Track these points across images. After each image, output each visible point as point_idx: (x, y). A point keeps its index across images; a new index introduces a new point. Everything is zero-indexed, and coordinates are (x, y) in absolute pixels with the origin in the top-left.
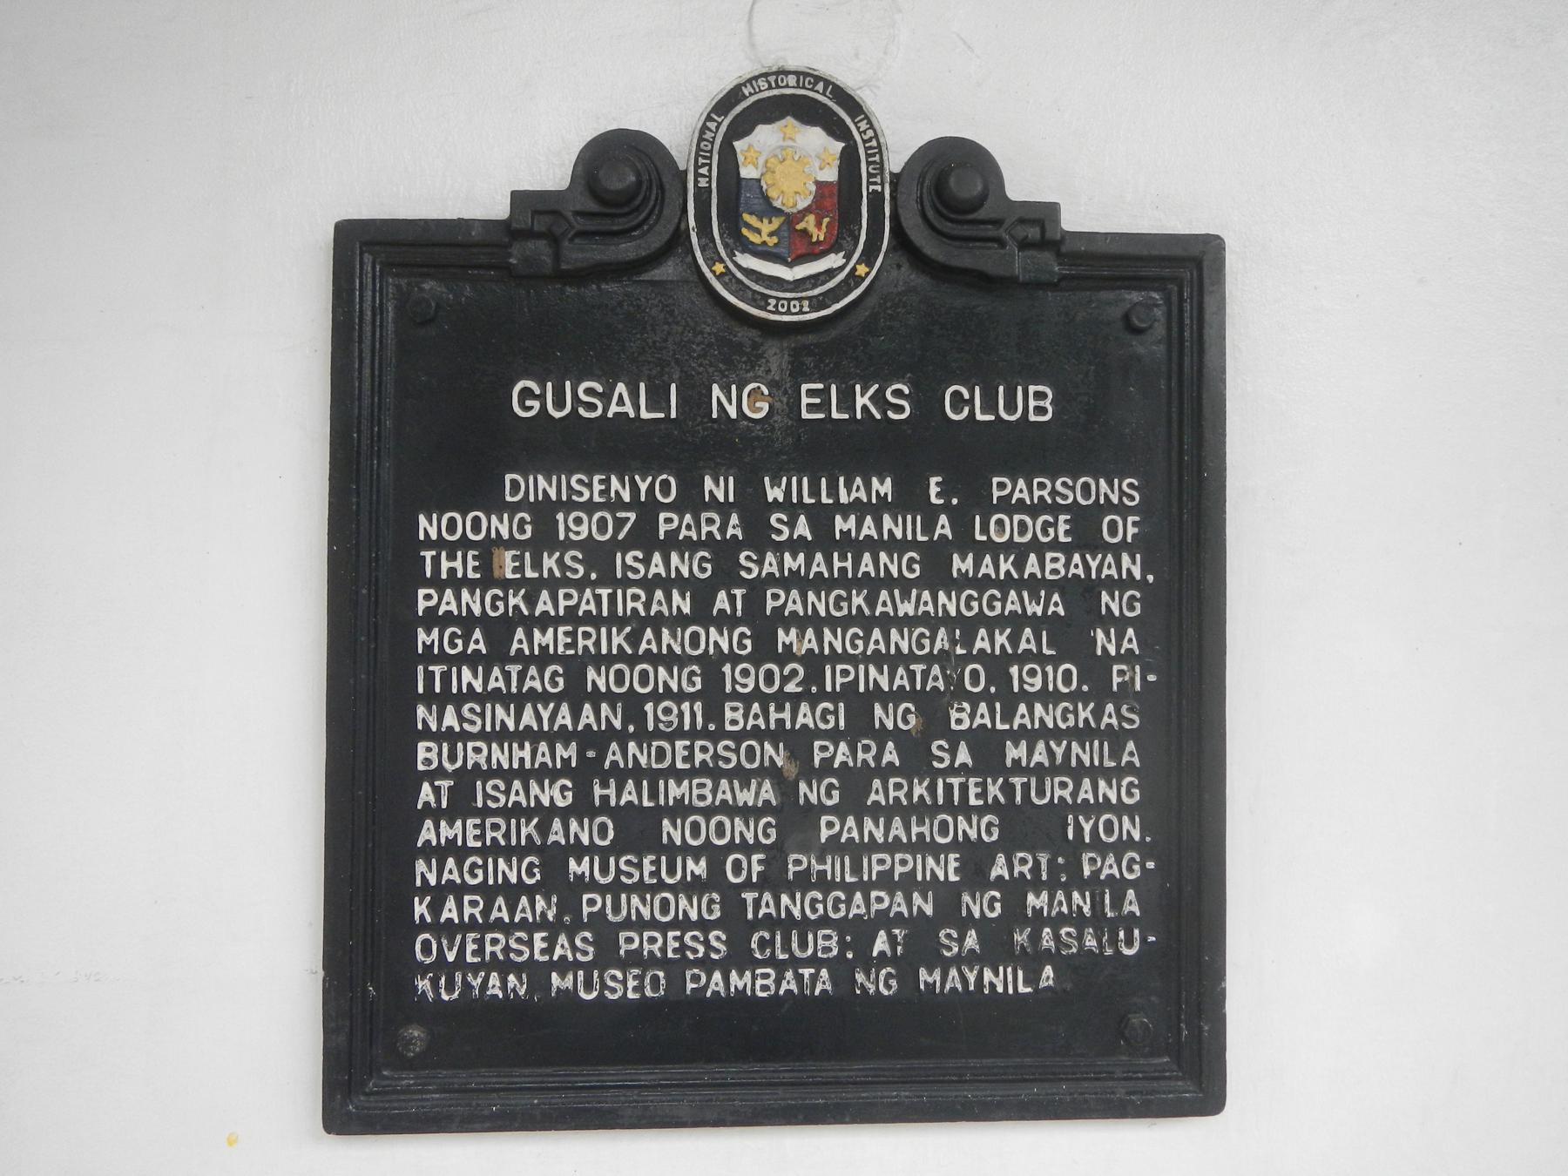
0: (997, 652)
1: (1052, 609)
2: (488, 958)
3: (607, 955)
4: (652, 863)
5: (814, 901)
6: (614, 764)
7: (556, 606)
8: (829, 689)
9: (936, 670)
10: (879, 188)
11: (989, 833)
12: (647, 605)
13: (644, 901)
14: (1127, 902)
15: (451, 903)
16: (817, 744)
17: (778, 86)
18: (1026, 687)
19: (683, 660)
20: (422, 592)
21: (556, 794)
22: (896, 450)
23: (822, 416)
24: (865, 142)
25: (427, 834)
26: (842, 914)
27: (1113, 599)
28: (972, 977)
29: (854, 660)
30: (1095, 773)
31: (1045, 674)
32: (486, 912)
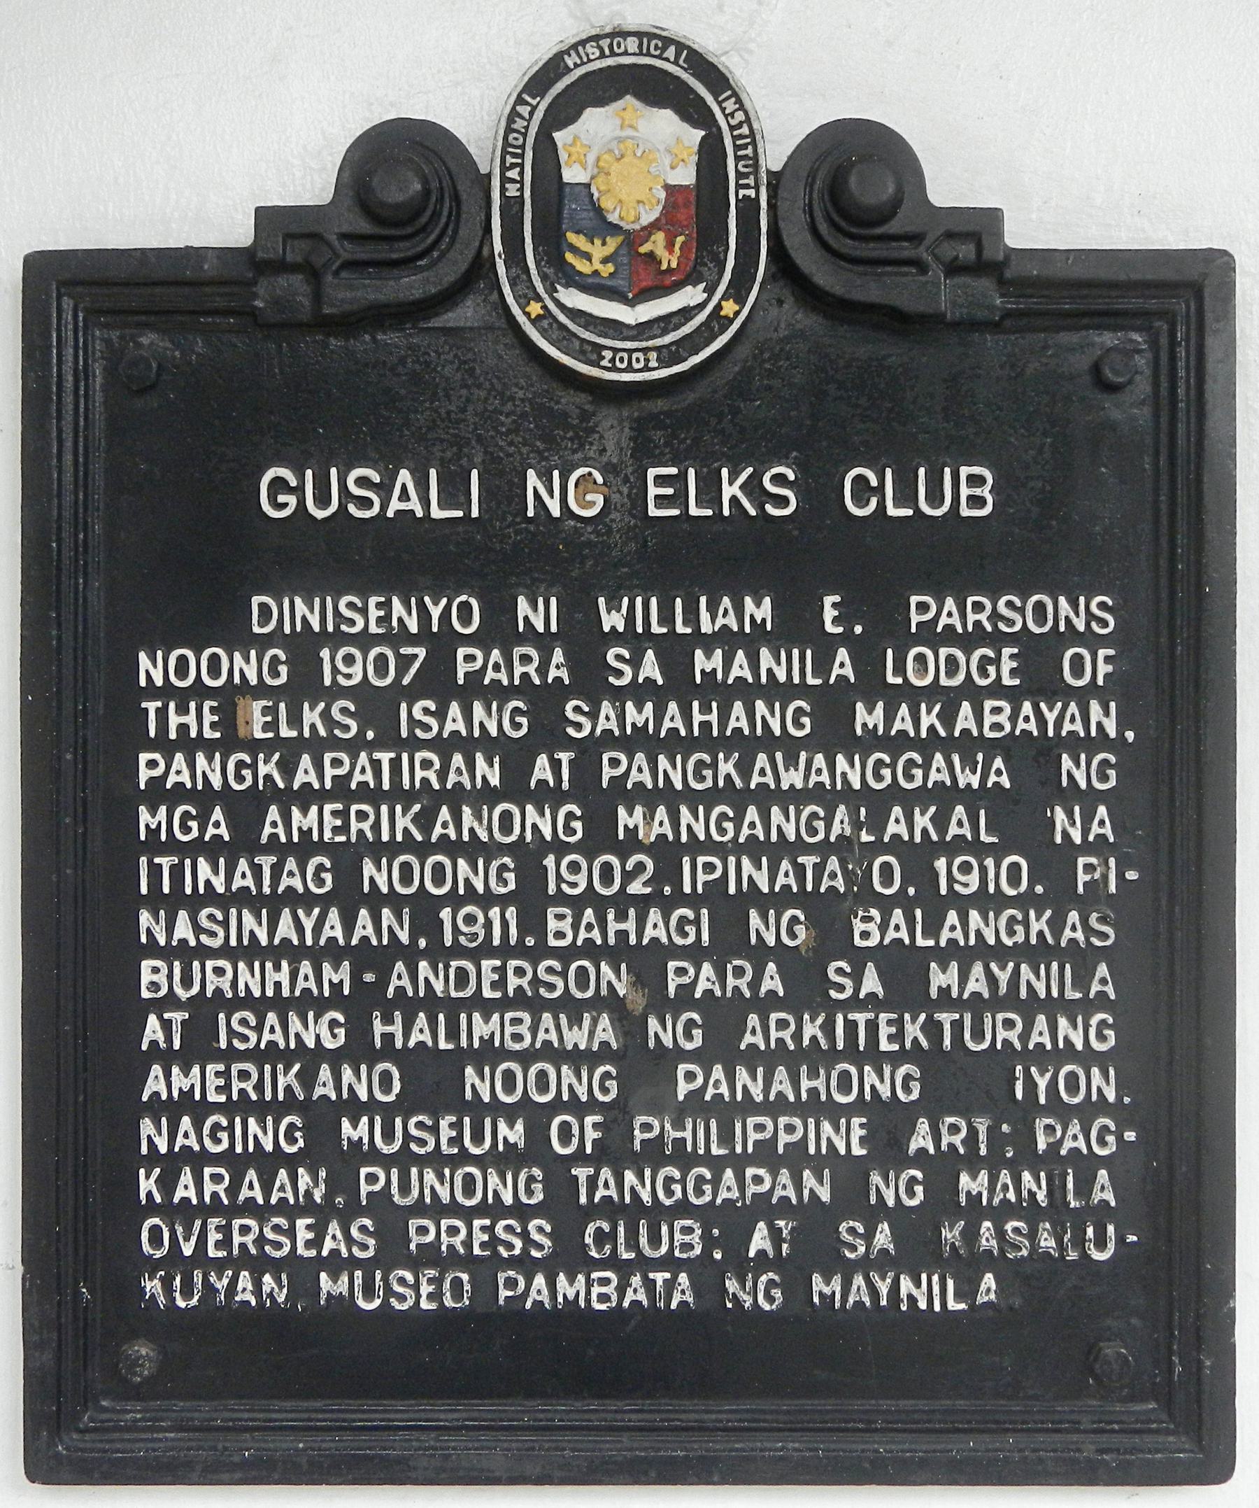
0: (918, 839)
1: (992, 779)
2: (236, 1252)
3: (393, 1250)
4: (451, 1126)
5: (669, 1180)
6: (400, 990)
7: (321, 777)
8: (687, 889)
9: (833, 864)
10: (752, 193)
11: (907, 1089)
12: (443, 775)
13: (441, 1177)
14: (1097, 1187)
15: (187, 1177)
16: (672, 965)
17: (613, 54)
18: (957, 887)
19: (490, 850)
20: (144, 758)
21: (323, 1032)
23: (675, 512)
24: (732, 128)
25: (155, 1084)
26: (707, 1198)
27: (1078, 765)
28: (884, 1288)
29: (721, 850)
30: (1053, 1007)
31: (983, 870)
32: (233, 1190)
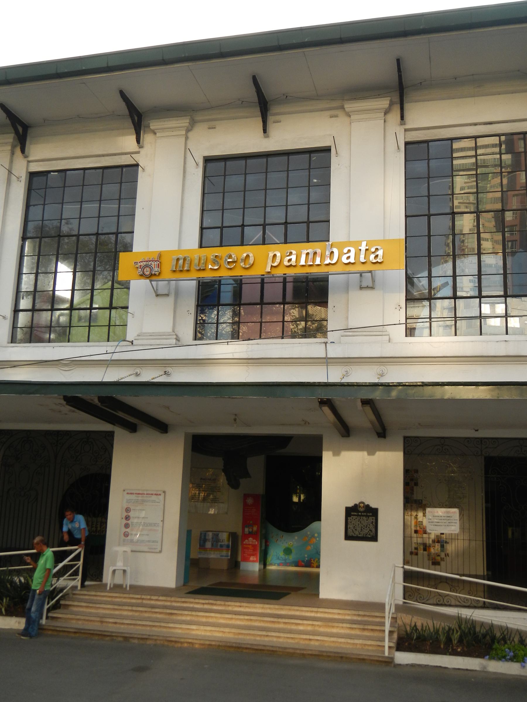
22: (366, 516)
